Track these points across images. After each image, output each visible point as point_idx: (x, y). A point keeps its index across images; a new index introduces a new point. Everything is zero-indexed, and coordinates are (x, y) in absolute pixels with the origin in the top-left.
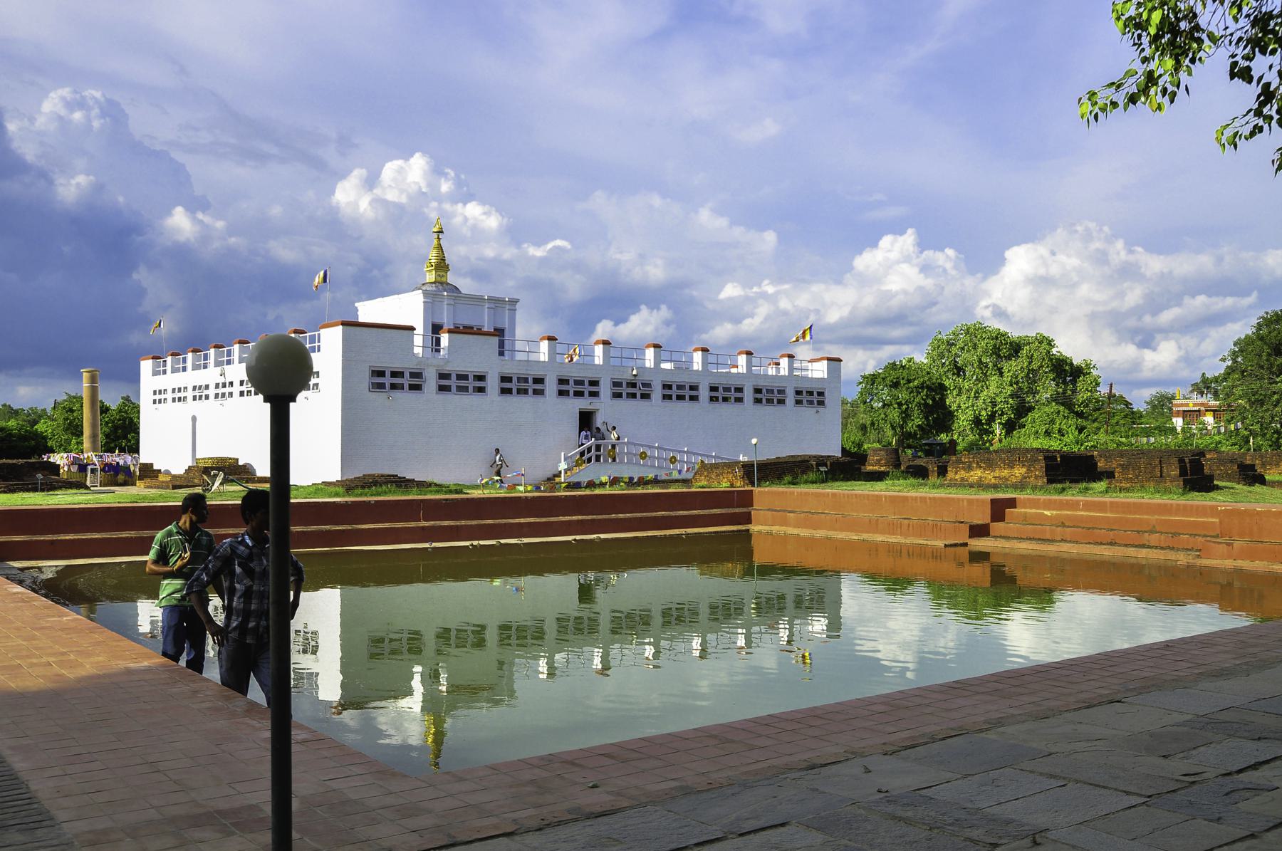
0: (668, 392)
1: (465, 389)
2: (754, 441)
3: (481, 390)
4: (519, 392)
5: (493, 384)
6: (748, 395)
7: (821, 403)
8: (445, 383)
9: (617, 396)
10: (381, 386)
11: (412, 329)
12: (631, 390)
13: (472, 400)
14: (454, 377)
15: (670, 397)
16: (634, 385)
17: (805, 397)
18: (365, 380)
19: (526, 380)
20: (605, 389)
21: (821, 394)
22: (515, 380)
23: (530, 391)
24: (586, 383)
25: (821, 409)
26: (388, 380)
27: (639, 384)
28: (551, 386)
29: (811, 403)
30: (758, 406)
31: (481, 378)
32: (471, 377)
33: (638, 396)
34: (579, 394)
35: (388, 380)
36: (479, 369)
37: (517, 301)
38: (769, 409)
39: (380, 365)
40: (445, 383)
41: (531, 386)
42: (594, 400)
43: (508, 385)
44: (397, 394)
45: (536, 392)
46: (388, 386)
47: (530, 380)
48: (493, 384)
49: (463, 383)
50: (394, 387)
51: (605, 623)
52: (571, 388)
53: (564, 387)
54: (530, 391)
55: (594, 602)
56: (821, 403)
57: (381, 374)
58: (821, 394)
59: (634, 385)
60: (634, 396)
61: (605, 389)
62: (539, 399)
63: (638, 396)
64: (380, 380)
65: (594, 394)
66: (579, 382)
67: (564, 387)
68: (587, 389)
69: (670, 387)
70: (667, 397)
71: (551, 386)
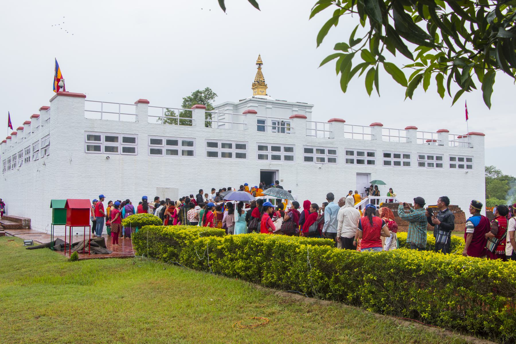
0: (350, 157)
1: (175, 152)
3: (190, 153)
4: (224, 155)
6: (414, 160)
7: (469, 167)
10: (97, 148)
15: (352, 161)
16: (322, 152)
18: (82, 143)
19: (230, 146)
22: (220, 145)
24: (282, 149)
28: (252, 151)
29: (461, 167)
40: (156, 147)
41: (234, 151)
45: (239, 156)
59: (322, 152)
60: (322, 160)
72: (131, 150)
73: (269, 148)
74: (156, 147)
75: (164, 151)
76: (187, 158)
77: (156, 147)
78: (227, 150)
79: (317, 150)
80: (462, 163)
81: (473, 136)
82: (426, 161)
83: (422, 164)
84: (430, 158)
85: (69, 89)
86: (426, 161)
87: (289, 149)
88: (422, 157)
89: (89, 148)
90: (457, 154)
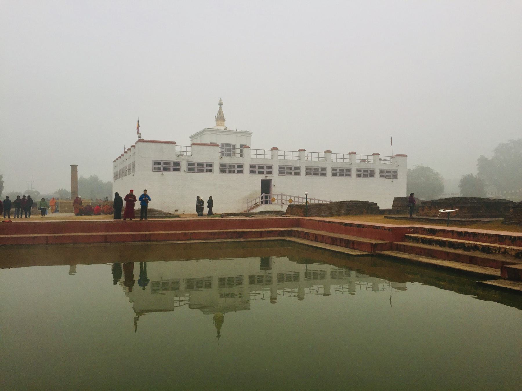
2: (306, 193)
3: (211, 171)
4: (230, 171)
5: (216, 168)
6: (354, 173)
7: (395, 177)
8: (192, 167)
9: (281, 173)
10: (159, 169)
11: (175, 143)
12: (289, 171)
13: (206, 175)
14: (196, 165)
15: (310, 174)
17: (386, 174)
18: (151, 166)
20: (275, 170)
21: (395, 172)
22: (227, 166)
23: (236, 171)
25: (394, 180)
26: (162, 166)
27: (313, 169)
28: (247, 169)
29: (388, 177)
30: (359, 178)
31: (211, 165)
32: (205, 165)
33: (293, 173)
34: (260, 172)
35: (162, 166)
36: (209, 161)
37: (251, 133)
38: (365, 180)
39: (158, 158)
40: (192, 167)
41: (236, 169)
42: (268, 175)
43: (223, 169)
44: (166, 173)
45: (239, 172)
46: (162, 168)
47: (236, 166)
48: (216, 168)
49: (200, 167)
50: (165, 169)
51: (275, 279)
52: (257, 169)
53: (253, 169)
54: (236, 171)
55: (270, 269)
56: (395, 177)
57: (159, 163)
58: (395, 172)
60: (291, 173)
61: (275, 170)
62: (240, 175)
63: (293, 173)
64: (159, 166)
65: (270, 173)
66: (261, 167)
67: (253, 169)
68: (265, 170)
69: (310, 169)
70: (308, 174)
71: (247, 169)
72: (177, 170)
73: (257, 167)
74: (191, 167)
75: (196, 169)
76: (209, 174)
77: (191, 167)
78: (232, 168)
79: (288, 168)
80: (389, 174)
81: (398, 157)
82: (362, 173)
83: (359, 175)
84: (364, 171)
85: (144, 137)
86: (362, 173)
87: (270, 167)
88: (360, 171)
89: (154, 168)
90: (385, 168)
